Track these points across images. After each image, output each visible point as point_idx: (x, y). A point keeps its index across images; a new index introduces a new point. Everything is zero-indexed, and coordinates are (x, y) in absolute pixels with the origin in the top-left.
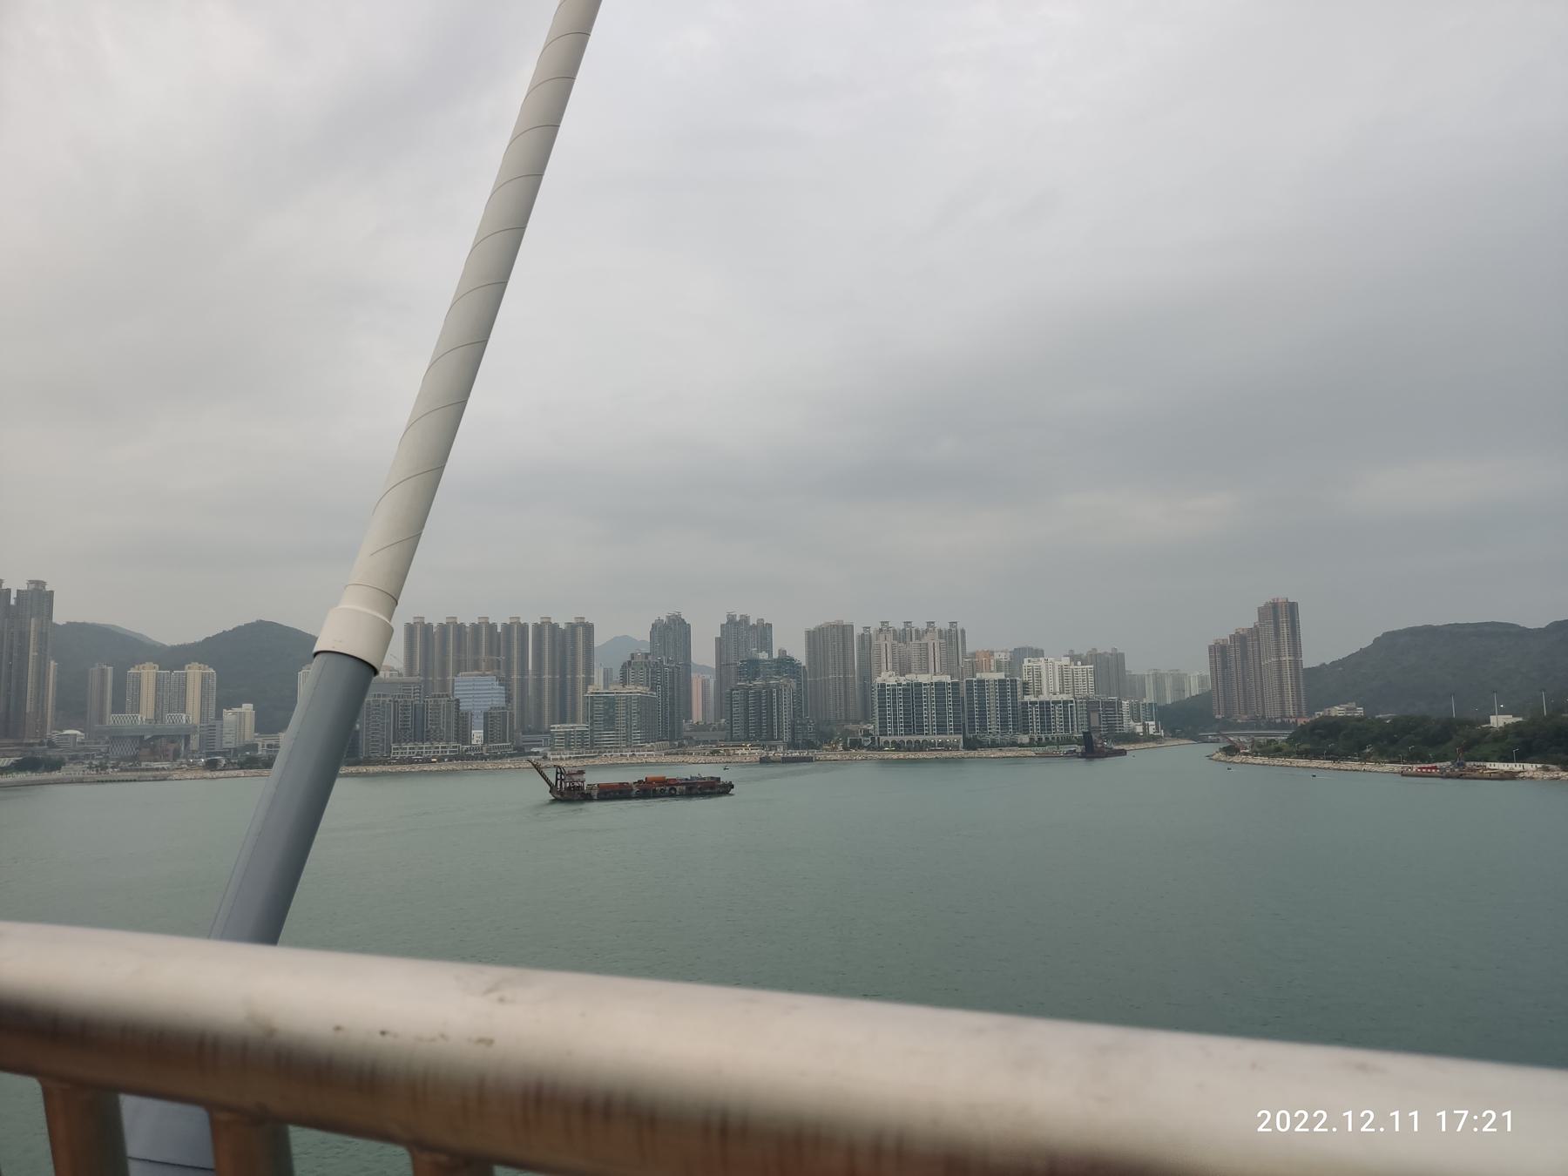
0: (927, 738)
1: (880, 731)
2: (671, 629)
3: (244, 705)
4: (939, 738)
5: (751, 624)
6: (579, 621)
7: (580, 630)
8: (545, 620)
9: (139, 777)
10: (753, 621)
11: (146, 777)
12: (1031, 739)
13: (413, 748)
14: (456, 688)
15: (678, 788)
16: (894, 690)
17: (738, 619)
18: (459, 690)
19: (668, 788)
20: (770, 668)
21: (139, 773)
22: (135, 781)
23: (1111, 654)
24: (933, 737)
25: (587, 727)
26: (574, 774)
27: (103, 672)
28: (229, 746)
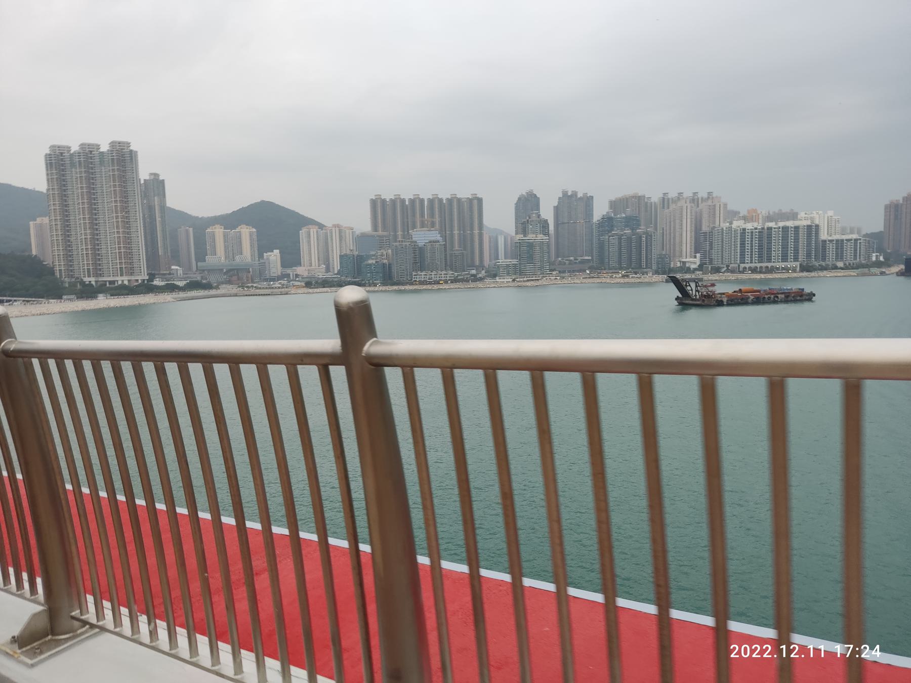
0: (772, 264)
1: (740, 261)
3: (274, 250)
4: (783, 265)
5: (579, 196)
7: (475, 202)
8: (453, 196)
9: (272, 292)
10: (580, 195)
11: (275, 292)
12: (845, 264)
13: (426, 275)
15: (779, 296)
16: (752, 232)
17: (569, 194)
19: (772, 296)
20: (621, 223)
21: (271, 290)
22: (269, 295)
23: (790, 213)
24: (778, 263)
25: (517, 262)
26: (709, 286)
27: (187, 231)
28: (274, 275)
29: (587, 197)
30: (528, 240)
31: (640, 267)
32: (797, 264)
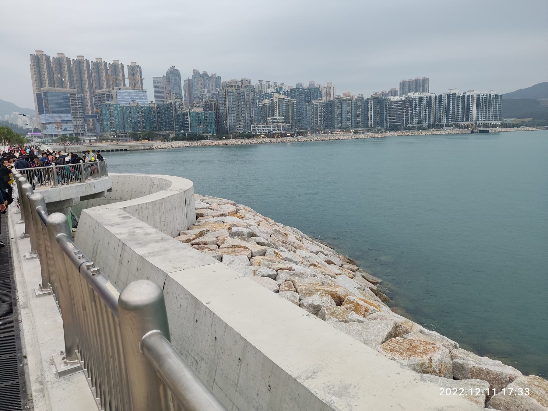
4: (494, 122)
6: (134, 64)
9: (130, 147)
10: (210, 75)
11: (135, 146)
14: (118, 97)
16: (483, 97)
17: (201, 73)
18: (119, 98)
29: (217, 77)
30: (286, 99)
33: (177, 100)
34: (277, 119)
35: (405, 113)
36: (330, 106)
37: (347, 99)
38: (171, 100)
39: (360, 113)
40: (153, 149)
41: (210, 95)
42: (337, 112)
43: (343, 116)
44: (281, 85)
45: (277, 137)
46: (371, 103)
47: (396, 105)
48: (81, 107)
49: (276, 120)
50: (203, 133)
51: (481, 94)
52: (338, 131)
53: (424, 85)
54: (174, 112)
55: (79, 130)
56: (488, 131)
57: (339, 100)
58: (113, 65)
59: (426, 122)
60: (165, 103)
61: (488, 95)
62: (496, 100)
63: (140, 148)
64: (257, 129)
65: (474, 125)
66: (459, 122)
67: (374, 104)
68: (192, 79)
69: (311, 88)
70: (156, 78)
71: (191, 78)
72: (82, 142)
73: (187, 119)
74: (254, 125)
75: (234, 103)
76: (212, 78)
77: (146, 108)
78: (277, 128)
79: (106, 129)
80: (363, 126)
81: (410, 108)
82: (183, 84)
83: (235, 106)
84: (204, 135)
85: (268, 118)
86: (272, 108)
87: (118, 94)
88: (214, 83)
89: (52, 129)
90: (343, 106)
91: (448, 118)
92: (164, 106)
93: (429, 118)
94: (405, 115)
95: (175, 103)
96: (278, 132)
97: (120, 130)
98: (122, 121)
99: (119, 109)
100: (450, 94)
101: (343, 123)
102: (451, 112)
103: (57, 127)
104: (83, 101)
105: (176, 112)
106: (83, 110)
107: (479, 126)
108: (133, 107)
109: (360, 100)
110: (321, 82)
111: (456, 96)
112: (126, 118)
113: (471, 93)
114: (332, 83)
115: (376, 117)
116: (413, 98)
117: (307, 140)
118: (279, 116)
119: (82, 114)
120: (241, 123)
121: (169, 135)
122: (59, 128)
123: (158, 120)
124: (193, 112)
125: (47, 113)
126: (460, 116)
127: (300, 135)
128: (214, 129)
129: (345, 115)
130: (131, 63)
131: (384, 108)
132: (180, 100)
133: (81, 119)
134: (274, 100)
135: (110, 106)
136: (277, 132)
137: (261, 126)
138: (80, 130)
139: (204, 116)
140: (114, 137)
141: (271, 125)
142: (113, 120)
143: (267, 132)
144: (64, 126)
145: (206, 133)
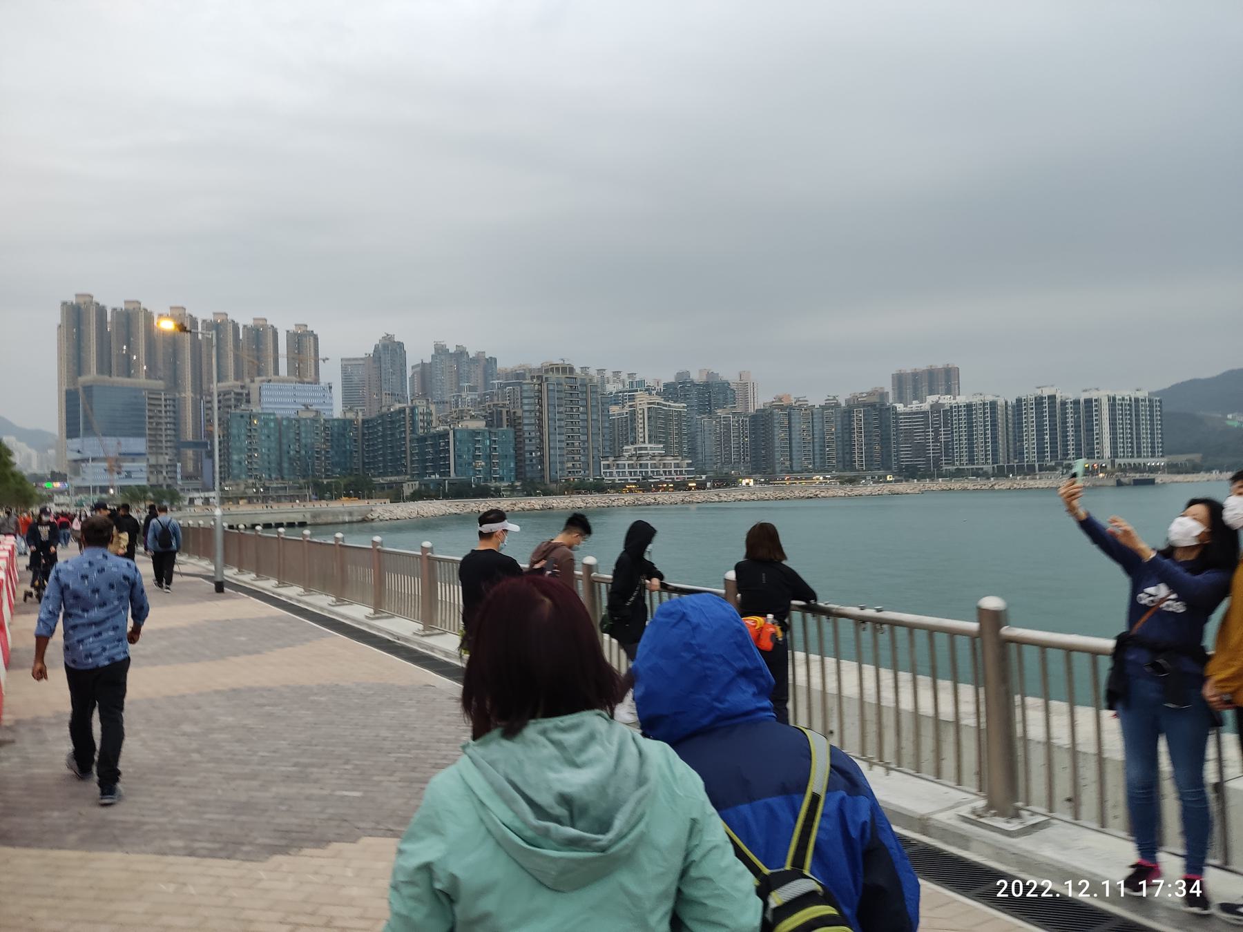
2: (397, 353)
4: (1152, 462)
5: (471, 357)
6: (303, 328)
8: (261, 323)
9: (314, 515)
11: (326, 513)
14: (264, 399)
16: (1122, 404)
17: (452, 350)
18: (270, 403)
29: (487, 359)
31: (849, 465)
32: (1162, 462)
33: (417, 402)
34: (649, 448)
35: (931, 441)
36: (761, 423)
37: (800, 405)
38: (400, 402)
39: (832, 437)
40: (373, 520)
41: (477, 397)
42: (780, 435)
43: (794, 445)
44: (629, 378)
45: (666, 489)
46: (859, 415)
47: (910, 418)
48: (170, 423)
49: (646, 452)
50: (486, 480)
51: (1117, 397)
52: (783, 479)
53: (948, 380)
54: (408, 432)
55: (161, 477)
56: (1151, 482)
57: (782, 408)
58: (253, 330)
59: (987, 459)
60: (384, 410)
61: (1133, 399)
62: (1151, 411)
63: (341, 519)
64: (615, 471)
65: (1109, 467)
66: (1070, 459)
67: (866, 417)
68: (430, 364)
69: (710, 383)
70: (349, 360)
71: (428, 360)
72: (186, 503)
73: (444, 446)
74: (607, 462)
75: (562, 409)
76: (475, 361)
77: (336, 424)
78: (662, 470)
79: (236, 472)
80: (841, 466)
81: (942, 429)
82: (409, 373)
83: (563, 416)
84: (489, 484)
85: (625, 448)
86: (631, 425)
87: (264, 393)
88: (480, 371)
89: (95, 475)
90: (793, 421)
91: (1041, 451)
92: (382, 416)
93: (995, 452)
94: (931, 444)
95: (413, 409)
96: (666, 479)
97: (270, 476)
98: (277, 453)
99: (272, 425)
100: (1042, 398)
101: (794, 461)
102: (1047, 437)
103: (109, 470)
104: (176, 407)
105: (413, 432)
106: (174, 430)
107: (1124, 469)
108: (305, 419)
109: (832, 408)
110: (728, 374)
111: (1058, 401)
112: (285, 447)
113: (1094, 395)
114: (749, 372)
115: (871, 446)
116: (951, 407)
117: (740, 497)
118: (650, 442)
119: (172, 438)
120: (577, 457)
121: (400, 484)
122: (113, 470)
123: (363, 450)
124: (462, 431)
125: (85, 435)
126: (1070, 447)
127: (719, 487)
128: (511, 471)
129: (799, 443)
130: (296, 325)
131: (890, 426)
132: (425, 403)
133: (169, 451)
134: (638, 405)
135: (251, 416)
136: (663, 478)
137: (625, 465)
138: (165, 477)
139: (490, 439)
140: (258, 491)
141: (649, 462)
142: (256, 450)
143: (640, 478)
144: (127, 466)
145: (493, 481)
